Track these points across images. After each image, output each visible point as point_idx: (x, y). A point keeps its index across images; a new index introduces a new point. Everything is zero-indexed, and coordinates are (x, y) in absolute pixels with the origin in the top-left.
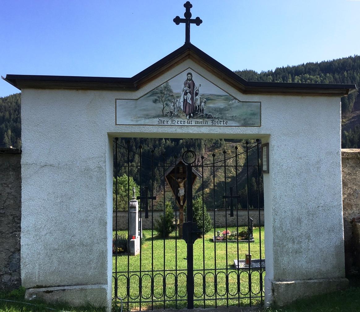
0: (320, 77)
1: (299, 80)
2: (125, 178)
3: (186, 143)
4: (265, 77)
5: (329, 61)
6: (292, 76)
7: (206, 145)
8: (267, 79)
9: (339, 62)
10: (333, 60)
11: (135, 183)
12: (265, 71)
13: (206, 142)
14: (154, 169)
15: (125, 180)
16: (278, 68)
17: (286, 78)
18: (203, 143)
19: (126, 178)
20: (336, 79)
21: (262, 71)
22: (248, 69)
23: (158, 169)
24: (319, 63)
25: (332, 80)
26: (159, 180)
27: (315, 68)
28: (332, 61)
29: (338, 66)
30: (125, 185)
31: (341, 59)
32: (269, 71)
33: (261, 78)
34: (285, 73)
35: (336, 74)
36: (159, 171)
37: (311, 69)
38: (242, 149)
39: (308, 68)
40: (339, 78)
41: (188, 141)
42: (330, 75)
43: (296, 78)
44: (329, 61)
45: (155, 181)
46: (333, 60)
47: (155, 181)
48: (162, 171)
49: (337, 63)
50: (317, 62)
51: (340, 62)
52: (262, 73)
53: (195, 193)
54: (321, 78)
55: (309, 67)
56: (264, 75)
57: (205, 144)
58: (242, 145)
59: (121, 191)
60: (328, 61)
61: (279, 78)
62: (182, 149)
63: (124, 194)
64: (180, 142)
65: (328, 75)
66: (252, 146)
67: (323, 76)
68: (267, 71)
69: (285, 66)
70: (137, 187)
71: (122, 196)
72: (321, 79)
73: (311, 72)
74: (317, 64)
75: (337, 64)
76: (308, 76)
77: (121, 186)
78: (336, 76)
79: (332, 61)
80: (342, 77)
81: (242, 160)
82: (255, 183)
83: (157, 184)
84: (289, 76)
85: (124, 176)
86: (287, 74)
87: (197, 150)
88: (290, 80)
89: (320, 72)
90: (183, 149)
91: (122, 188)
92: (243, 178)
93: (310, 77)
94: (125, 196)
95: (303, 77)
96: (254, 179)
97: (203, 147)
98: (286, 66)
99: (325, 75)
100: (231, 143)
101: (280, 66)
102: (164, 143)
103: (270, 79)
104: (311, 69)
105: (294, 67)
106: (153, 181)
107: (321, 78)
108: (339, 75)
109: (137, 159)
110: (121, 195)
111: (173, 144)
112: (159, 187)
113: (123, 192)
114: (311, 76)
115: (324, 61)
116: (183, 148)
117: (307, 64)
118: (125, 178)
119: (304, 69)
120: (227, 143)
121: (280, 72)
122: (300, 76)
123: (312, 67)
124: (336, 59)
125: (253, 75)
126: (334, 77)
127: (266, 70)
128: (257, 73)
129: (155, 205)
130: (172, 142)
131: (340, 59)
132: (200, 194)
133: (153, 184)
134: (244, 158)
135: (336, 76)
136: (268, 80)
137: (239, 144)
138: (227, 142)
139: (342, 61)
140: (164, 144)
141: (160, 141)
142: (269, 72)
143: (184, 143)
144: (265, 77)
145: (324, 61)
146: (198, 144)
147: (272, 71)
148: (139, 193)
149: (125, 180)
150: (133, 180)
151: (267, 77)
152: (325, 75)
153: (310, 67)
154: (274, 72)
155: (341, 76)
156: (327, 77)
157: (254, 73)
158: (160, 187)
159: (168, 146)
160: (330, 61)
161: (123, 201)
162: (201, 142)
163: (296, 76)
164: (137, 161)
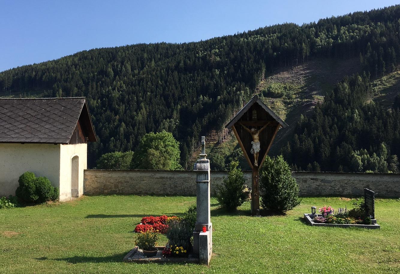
0: (370, 26)
1: (345, 31)
2: (164, 134)
3: (224, 99)
4: (308, 29)
5: (379, 9)
6: (337, 27)
7: (244, 101)
8: (309, 32)
9: (391, 9)
10: (385, 7)
11: (174, 139)
12: (307, 23)
13: (244, 98)
14: (192, 126)
15: (164, 135)
16: (322, 19)
17: (331, 29)
18: (242, 99)
19: (166, 133)
20: (388, 28)
21: (304, 23)
22: (288, 23)
23: (196, 125)
24: (368, 11)
25: (385, 29)
26: (197, 136)
27: (363, 17)
28: (383, 8)
29: (390, 14)
30: (165, 140)
31: (393, 6)
32: (311, 23)
33: (302, 30)
34: (329, 24)
35: (388, 23)
36: (197, 127)
37: (359, 18)
38: (283, 105)
39: (356, 17)
40: (393, 26)
41: (226, 97)
42: (381, 24)
43: (342, 29)
44: (379, 9)
45: (193, 138)
46: (385, 7)
47: (193, 138)
48: (200, 127)
49: (390, 11)
50: (365, 11)
51: (393, 10)
52: (304, 25)
53: (234, 150)
54: (372, 28)
55: (357, 16)
56: (306, 27)
57: (243, 100)
58: (282, 100)
59: (161, 147)
60: (378, 10)
61: (323, 30)
62: (219, 105)
63: (164, 149)
64: (218, 98)
65: (379, 23)
66: (293, 101)
67: (374, 25)
68: (309, 23)
69: (329, 17)
70: (176, 143)
71: (161, 152)
72: (370, 29)
73: (359, 21)
74: (366, 13)
75: (389, 11)
76: (356, 26)
77: (161, 142)
78: (389, 24)
79: (383, 8)
80: (396, 26)
81: (282, 116)
82: (298, 140)
83: (195, 140)
84: (334, 27)
85: (163, 131)
86: (332, 25)
87: (235, 106)
88: (336, 31)
89: (370, 21)
90: (220, 105)
91: (162, 144)
92: (284, 135)
93: (358, 27)
94: (164, 152)
95: (350, 27)
96: (296, 136)
97: (241, 103)
98: (331, 17)
99: (376, 24)
100: (270, 98)
101: (324, 17)
102: (202, 99)
103: (313, 31)
104: (359, 18)
105: (339, 18)
106: (191, 137)
107: (372, 28)
108: (392, 24)
109: (176, 116)
110: (161, 150)
111: (211, 101)
112: (197, 143)
113: (162, 147)
114: (359, 26)
115: (374, 9)
116: (221, 104)
117: (354, 13)
118: (164, 134)
119: (350, 20)
120: (267, 99)
121: (324, 23)
122: (347, 26)
123: (360, 16)
124: (387, 6)
125: (293, 28)
126: (386, 26)
127: (308, 22)
128: (298, 25)
129: (193, 161)
130: (209, 99)
131: (393, 7)
132: (238, 151)
133: (191, 141)
134: (285, 114)
135: (389, 24)
136: (310, 32)
137: (279, 100)
138: (266, 98)
139: (395, 8)
140: (202, 101)
141: (198, 98)
142: (312, 24)
143: (222, 99)
144: (308, 29)
145: (374, 9)
146: (236, 100)
147: (314, 23)
148: (178, 149)
149: (164, 135)
150: (172, 136)
151: (309, 29)
152: (376, 24)
153: (358, 16)
154: (316, 23)
155: (395, 24)
156: (379, 26)
157: (295, 26)
158: (197, 143)
159: (206, 103)
160: (381, 8)
161: (162, 157)
162: (239, 98)
163: (342, 27)
164: (175, 117)
